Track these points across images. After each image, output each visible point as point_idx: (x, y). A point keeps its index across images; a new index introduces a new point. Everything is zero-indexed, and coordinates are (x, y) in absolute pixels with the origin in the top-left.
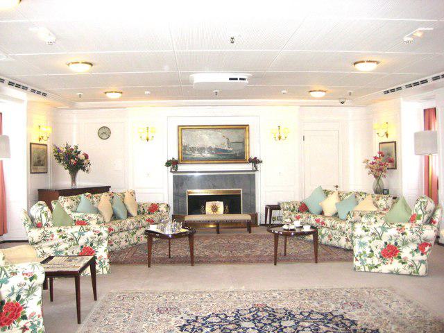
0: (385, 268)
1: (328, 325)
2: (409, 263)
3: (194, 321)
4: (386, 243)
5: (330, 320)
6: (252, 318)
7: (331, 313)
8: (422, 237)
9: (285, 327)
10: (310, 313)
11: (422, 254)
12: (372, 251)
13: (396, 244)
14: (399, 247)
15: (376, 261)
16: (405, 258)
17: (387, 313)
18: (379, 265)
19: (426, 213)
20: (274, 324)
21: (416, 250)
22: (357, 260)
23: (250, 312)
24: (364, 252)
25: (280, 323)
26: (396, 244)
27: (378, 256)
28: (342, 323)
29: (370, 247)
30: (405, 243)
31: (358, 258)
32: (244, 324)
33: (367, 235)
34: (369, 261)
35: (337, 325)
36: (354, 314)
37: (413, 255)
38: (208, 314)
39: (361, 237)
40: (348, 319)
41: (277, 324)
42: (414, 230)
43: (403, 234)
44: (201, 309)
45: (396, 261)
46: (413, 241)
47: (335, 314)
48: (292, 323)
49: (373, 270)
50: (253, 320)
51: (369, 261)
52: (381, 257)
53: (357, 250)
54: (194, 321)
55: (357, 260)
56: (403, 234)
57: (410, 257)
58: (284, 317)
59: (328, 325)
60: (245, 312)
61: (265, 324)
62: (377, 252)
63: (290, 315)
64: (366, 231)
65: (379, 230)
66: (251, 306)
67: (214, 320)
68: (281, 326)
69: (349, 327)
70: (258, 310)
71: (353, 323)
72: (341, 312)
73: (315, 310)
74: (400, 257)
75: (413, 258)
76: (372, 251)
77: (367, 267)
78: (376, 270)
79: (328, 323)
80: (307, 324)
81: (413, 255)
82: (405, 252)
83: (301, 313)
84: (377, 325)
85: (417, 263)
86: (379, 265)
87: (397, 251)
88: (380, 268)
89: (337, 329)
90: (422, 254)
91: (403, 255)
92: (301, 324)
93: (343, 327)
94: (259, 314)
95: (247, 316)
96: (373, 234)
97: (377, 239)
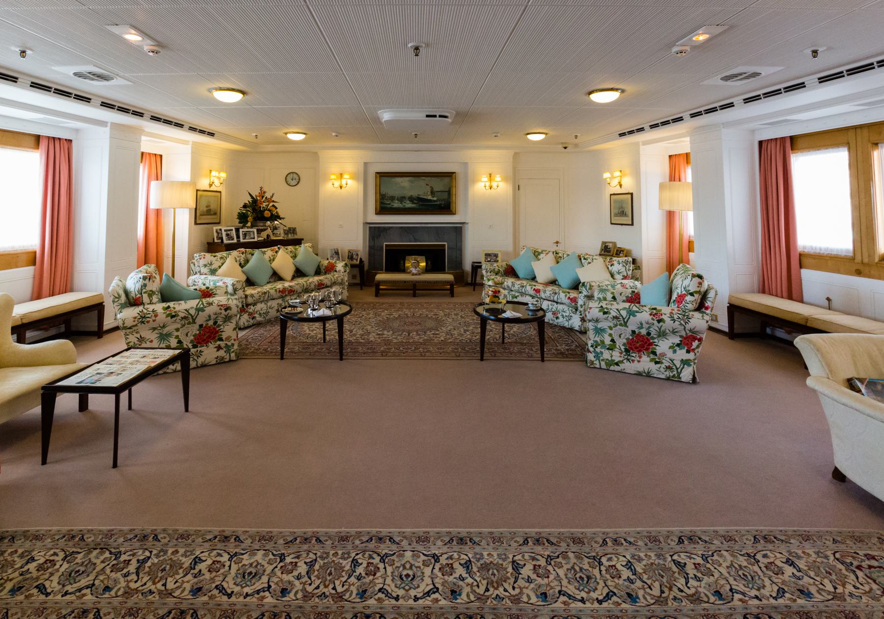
0: (629, 367)
2: (666, 363)
11: (688, 352)
12: (613, 341)
14: (653, 338)
15: (616, 356)
16: (663, 355)
18: (622, 362)
21: (678, 345)
24: (603, 342)
27: (623, 348)
29: (610, 335)
33: (606, 319)
34: (606, 355)
37: (675, 352)
39: (597, 321)
43: (659, 321)
45: (645, 359)
49: (612, 368)
51: (606, 355)
56: (659, 321)
62: (620, 343)
64: (605, 313)
74: (654, 353)
76: (613, 341)
77: (603, 363)
81: (675, 352)
82: (663, 346)
86: (622, 362)
87: (651, 344)
88: (622, 367)
90: (688, 352)
91: (659, 350)
96: (615, 318)
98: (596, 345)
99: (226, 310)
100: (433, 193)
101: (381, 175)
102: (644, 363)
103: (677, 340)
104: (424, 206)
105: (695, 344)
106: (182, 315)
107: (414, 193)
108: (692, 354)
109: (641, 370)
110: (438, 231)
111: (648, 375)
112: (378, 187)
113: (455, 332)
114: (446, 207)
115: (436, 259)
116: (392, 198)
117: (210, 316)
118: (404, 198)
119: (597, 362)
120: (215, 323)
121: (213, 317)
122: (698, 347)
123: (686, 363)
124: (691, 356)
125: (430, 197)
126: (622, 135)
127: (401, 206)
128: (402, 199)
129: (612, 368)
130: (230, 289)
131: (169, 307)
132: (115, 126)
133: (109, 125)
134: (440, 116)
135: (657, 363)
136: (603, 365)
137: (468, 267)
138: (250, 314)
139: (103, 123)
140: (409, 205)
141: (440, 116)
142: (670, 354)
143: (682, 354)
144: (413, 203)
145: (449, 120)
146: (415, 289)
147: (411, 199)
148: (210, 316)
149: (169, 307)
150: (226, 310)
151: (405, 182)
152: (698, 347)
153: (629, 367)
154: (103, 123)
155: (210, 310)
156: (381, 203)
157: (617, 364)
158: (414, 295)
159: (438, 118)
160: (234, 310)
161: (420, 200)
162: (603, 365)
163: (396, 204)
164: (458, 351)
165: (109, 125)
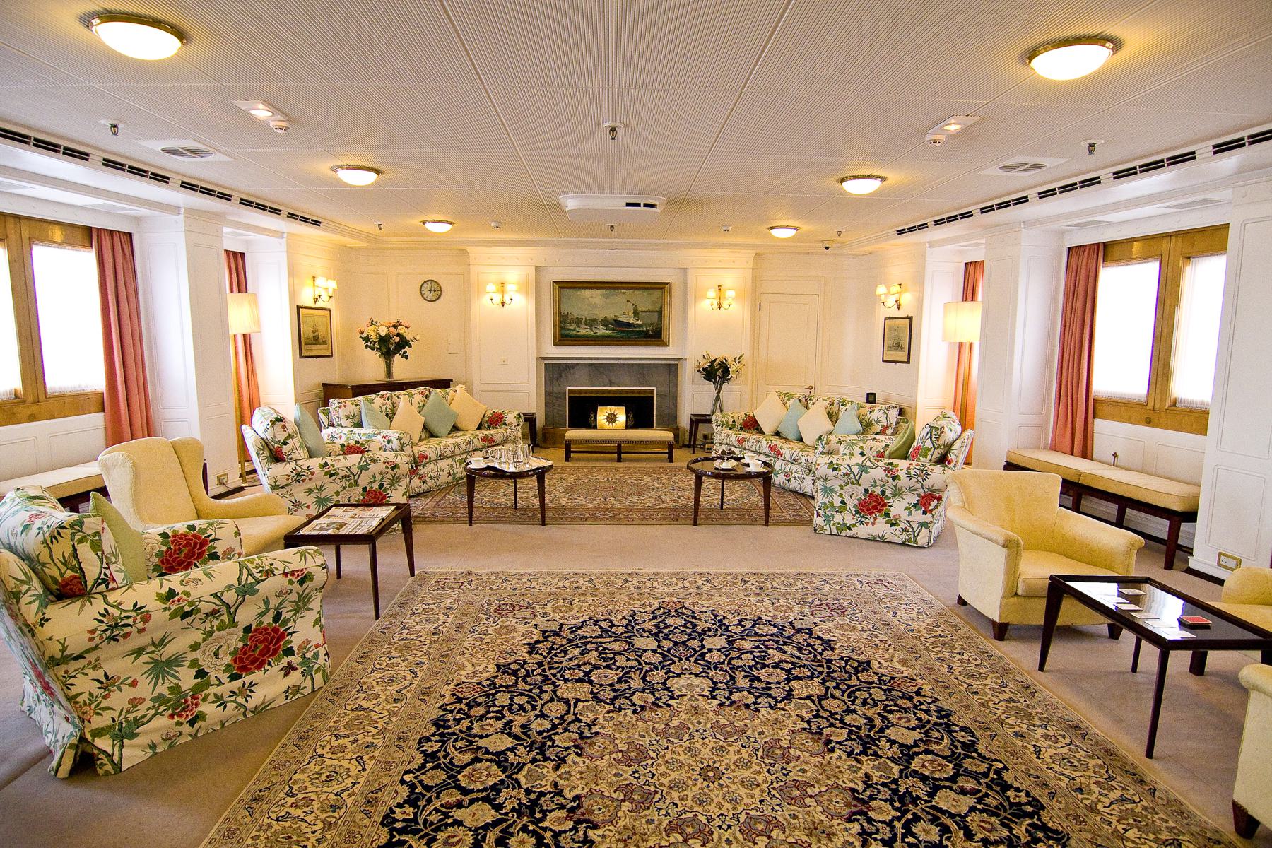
0: (862, 531)
1: (785, 648)
2: (903, 526)
3: (556, 634)
4: (866, 491)
5: (789, 638)
6: (654, 630)
7: (791, 623)
8: (926, 484)
9: (710, 650)
10: (756, 623)
11: (925, 513)
12: (843, 502)
13: (883, 493)
14: (888, 498)
16: (897, 517)
17: (887, 625)
18: (855, 525)
19: (939, 447)
20: (691, 643)
21: (915, 505)
22: (818, 515)
23: (654, 618)
24: (832, 504)
25: (702, 641)
26: (883, 493)
27: (853, 510)
28: (808, 645)
30: (898, 493)
31: (821, 512)
32: (640, 642)
34: (838, 518)
35: (800, 649)
36: (829, 628)
37: (910, 513)
38: (582, 619)
40: (819, 638)
41: (695, 644)
42: (913, 473)
44: (572, 610)
45: (881, 521)
46: (911, 490)
47: (798, 625)
48: (721, 642)
49: (844, 533)
50: (656, 634)
51: (838, 518)
52: (857, 512)
53: (820, 499)
54: (556, 634)
55: (818, 515)
57: (904, 516)
58: (709, 630)
59: (785, 648)
60: (646, 617)
61: (676, 643)
62: (851, 504)
63: (721, 625)
65: (856, 470)
66: (657, 605)
67: (590, 631)
68: (703, 647)
69: (821, 654)
70: (667, 613)
71: (829, 644)
72: (809, 621)
73: (764, 617)
74: (887, 515)
75: (909, 518)
76: (843, 502)
77: (834, 528)
78: (849, 533)
79: (785, 644)
80: (747, 645)
81: (910, 513)
82: (897, 508)
83: (739, 624)
84: (870, 651)
85: (915, 526)
86: (855, 525)
87: (884, 505)
88: (855, 530)
89: (798, 658)
90: (925, 513)
91: (893, 512)
92: (737, 644)
93: (810, 653)
94: (669, 621)
95: (647, 626)
97: (852, 483)
98: (824, 507)
99: (393, 468)
100: (636, 313)
101: (563, 286)
102: (879, 526)
103: (914, 500)
104: (624, 333)
105: (934, 503)
106: (342, 473)
107: (610, 314)
108: (929, 515)
109: (875, 534)
110: (642, 370)
111: (882, 540)
112: (557, 303)
113: (668, 498)
114: (655, 336)
115: (640, 411)
116: (578, 321)
117: (374, 477)
118: (595, 320)
119: (827, 527)
120: (381, 486)
121: (379, 477)
122: (936, 507)
123: (924, 525)
124: (928, 518)
125: (632, 321)
126: (901, 232)
127: (590, 332)
128: (591, 323)
129: (844, 533)
130: (395, 444)
131: (326, 464)
132: (191, 213)
133: (182, 211)
134: (646, 205)
135: (893, 525)
136: (834, 531)
137: (684, 422)
138: (421, 477)
139: (174, 209)
140: (601, 331)
141: (646, 205)
142: (904, 516)
143: (918, 516)
144: (608, 329)
145: (657, 210)
146: (619, 450)
147: (605, 323)
148: (374, 477)
149: (326, 464)
150: (393, 468)
151: (595, 296)
152: (936, 507)
153: (862, 531)
154: (174, 209)
155: (374, 468)
156: (562, 328)
157: (849, 528)
158: (619, 460)
159: (642, 208)
160: (405, 469)
161: (618, 324)
162: (834, 531)
163: (584, 331)
164: (672, 517)
165: (182, 211)
